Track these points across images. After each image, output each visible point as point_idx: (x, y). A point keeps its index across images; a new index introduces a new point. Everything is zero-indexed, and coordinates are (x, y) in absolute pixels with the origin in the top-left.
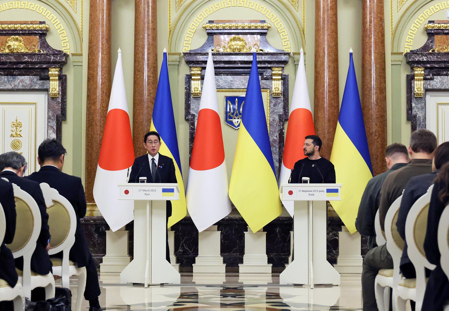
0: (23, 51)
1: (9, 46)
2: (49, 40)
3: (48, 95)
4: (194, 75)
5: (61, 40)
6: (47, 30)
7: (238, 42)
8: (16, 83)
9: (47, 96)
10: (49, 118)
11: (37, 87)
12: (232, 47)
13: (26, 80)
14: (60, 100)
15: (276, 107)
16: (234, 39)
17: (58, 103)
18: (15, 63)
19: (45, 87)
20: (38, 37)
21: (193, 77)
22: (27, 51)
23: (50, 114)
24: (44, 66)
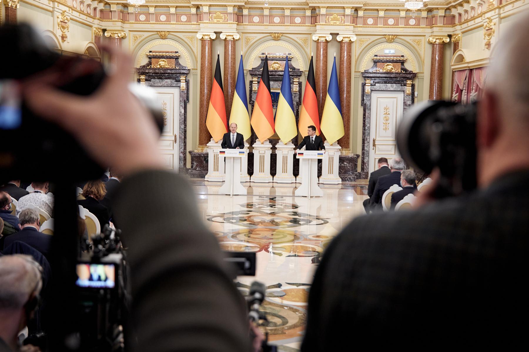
1: (160, 64)
2: (180, 61)
6: (179, 56)
10: (180, 101)
13: (169, 81)
18: (163, 73)
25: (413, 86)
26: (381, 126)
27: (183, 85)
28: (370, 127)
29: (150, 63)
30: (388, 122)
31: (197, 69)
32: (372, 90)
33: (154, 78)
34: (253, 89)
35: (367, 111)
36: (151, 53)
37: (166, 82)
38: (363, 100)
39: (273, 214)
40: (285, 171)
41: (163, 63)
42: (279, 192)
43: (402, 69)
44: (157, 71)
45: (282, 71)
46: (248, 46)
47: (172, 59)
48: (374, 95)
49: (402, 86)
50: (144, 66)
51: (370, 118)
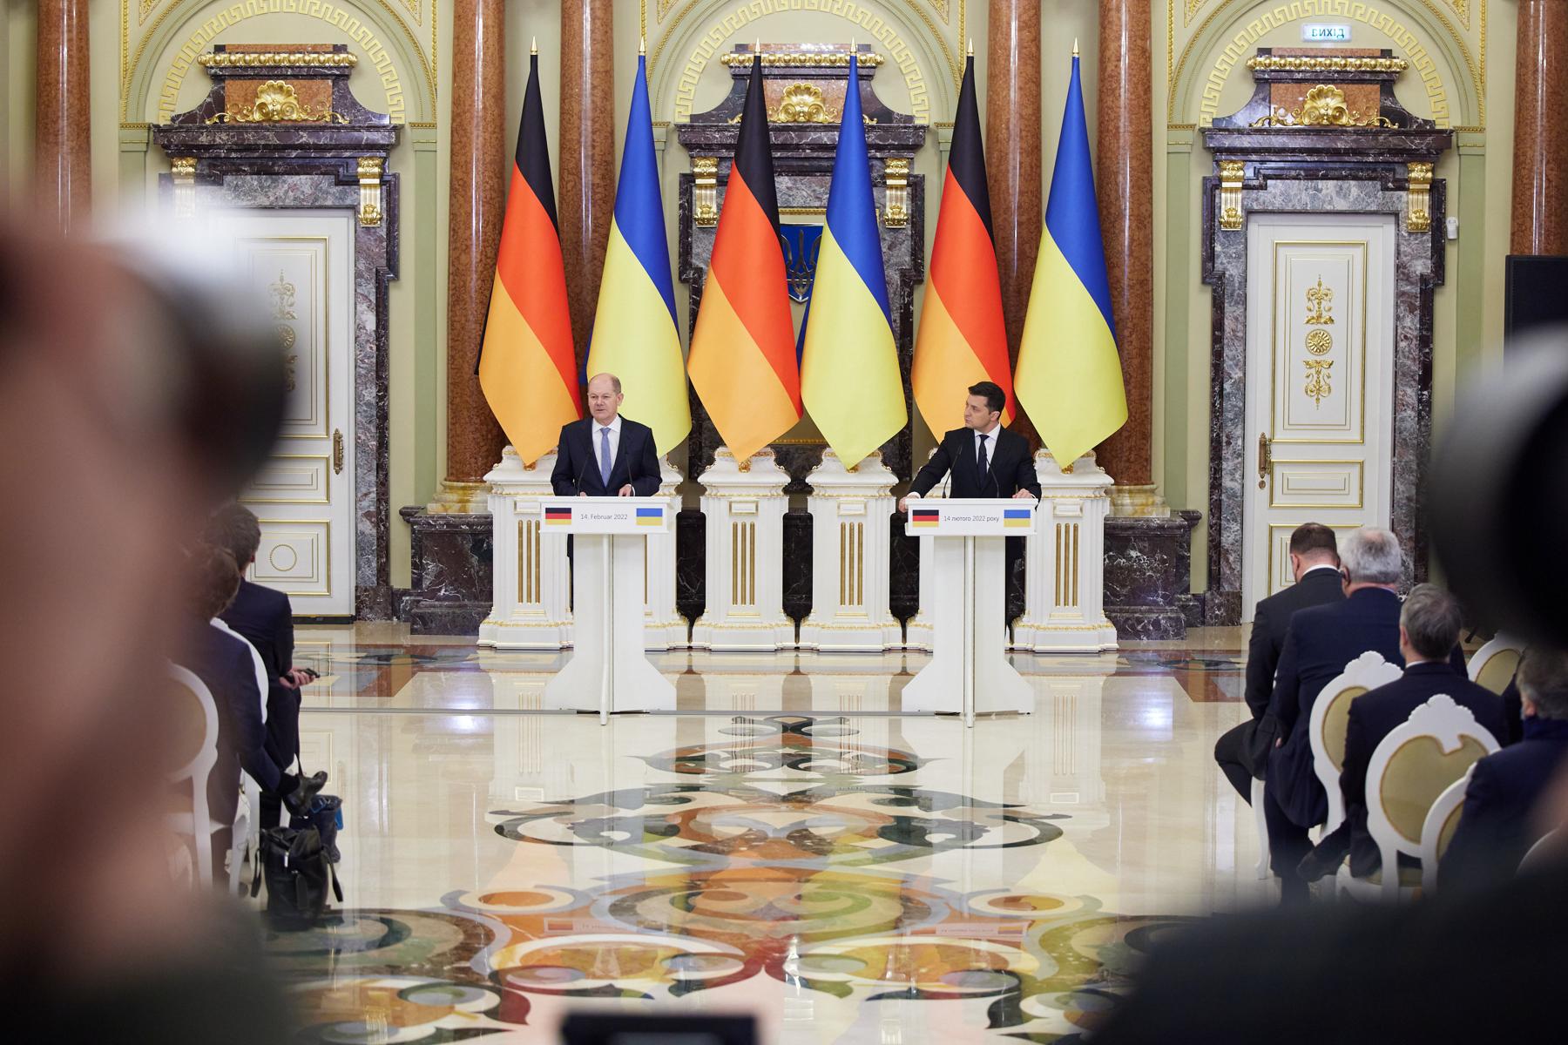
0: (295, 116)
1: (263, 105)
3: (356, 221)
4: (701, 175)
5: (387, 91)
6: (352, 65)
7: (806, 97)
8: (280, 193)
9: (352, 223)
10: (358, 275)
11: (329, 203)
12: (792, 110)
13: (304, 182)
14: (383, 233)
15: (895, 252)
16: (797, 91)
17: (380, 239)
18: (276, 148)
19: (348, 202)
20: (330, 82)
21: (698, 181)
22: (304, 116)
23: (362, 267)
24: (347, 154)
25: (1437, 190)
26: (1297, 377)
27: (370, 199)
28: (1243, 381)
29: (216, 103)
30: (1327, 358)
31: (434, 126)
32: (1249, 213)
33: (238, 171)
34: (698, 212)
35: (1229, 309)
36: (220, 57)
37: (294, 188)
38: (1209, 257)
39: (799, 799)
40: (851, 592)
41: (276, 100)
42: (825, 694)
43: (1384, 112)
44: (250, 137)
45: (829, 128)
46: (671, 15)
47: (317, 84)
48: (1262, 235)
49: (1385, 189)
50: (190, 117)
51: (1244, 340)
